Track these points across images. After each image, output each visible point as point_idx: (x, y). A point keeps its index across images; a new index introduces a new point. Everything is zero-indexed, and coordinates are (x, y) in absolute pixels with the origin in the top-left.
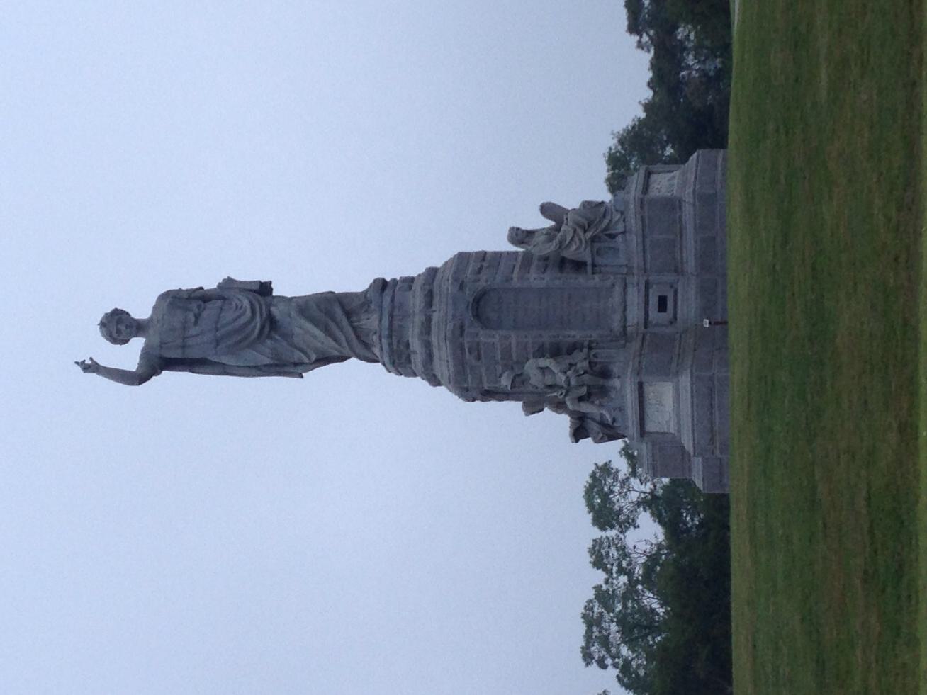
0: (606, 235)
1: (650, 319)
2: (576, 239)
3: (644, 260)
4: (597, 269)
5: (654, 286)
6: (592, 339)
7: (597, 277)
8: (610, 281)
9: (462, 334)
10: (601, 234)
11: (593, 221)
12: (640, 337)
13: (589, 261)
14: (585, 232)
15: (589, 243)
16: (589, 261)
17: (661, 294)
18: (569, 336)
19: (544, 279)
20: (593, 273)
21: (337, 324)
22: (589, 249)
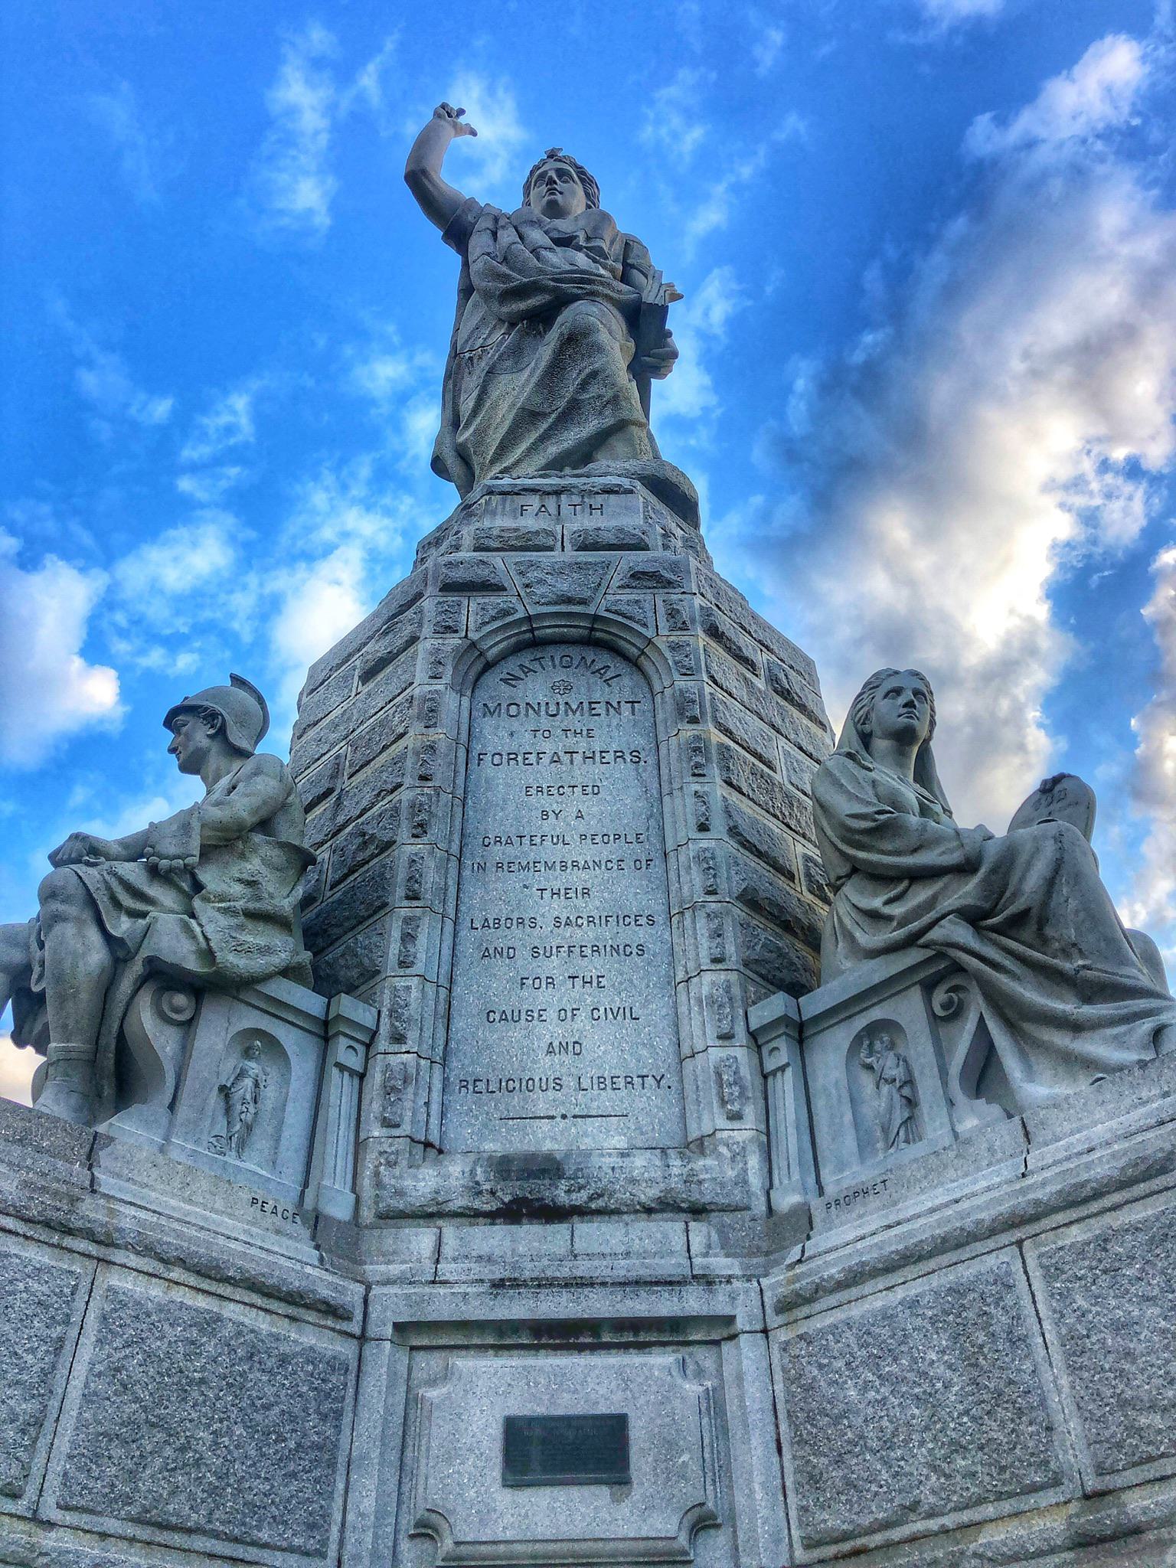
0: (981, 1019)
1: (464, 1363)
2: (921, 894)
3: (855, 1277)
4: (782, 1053)
5: (692, 1389)
6: (383, 1044)
7: (740, 1053)
8: (721, 1122)
9: (448, 588)
10: (977, 1005)
11: (1042, 942)
12: (324, 1283)
13: (813, 1004)
14: (973, 917)
15: (914, 956)
16: (813, 1004)
17: (638, 1434)
18: (408, 938)
19: (703, 828)
20: (756, 1039)
21: (543, 438)
22: (880, 970)
